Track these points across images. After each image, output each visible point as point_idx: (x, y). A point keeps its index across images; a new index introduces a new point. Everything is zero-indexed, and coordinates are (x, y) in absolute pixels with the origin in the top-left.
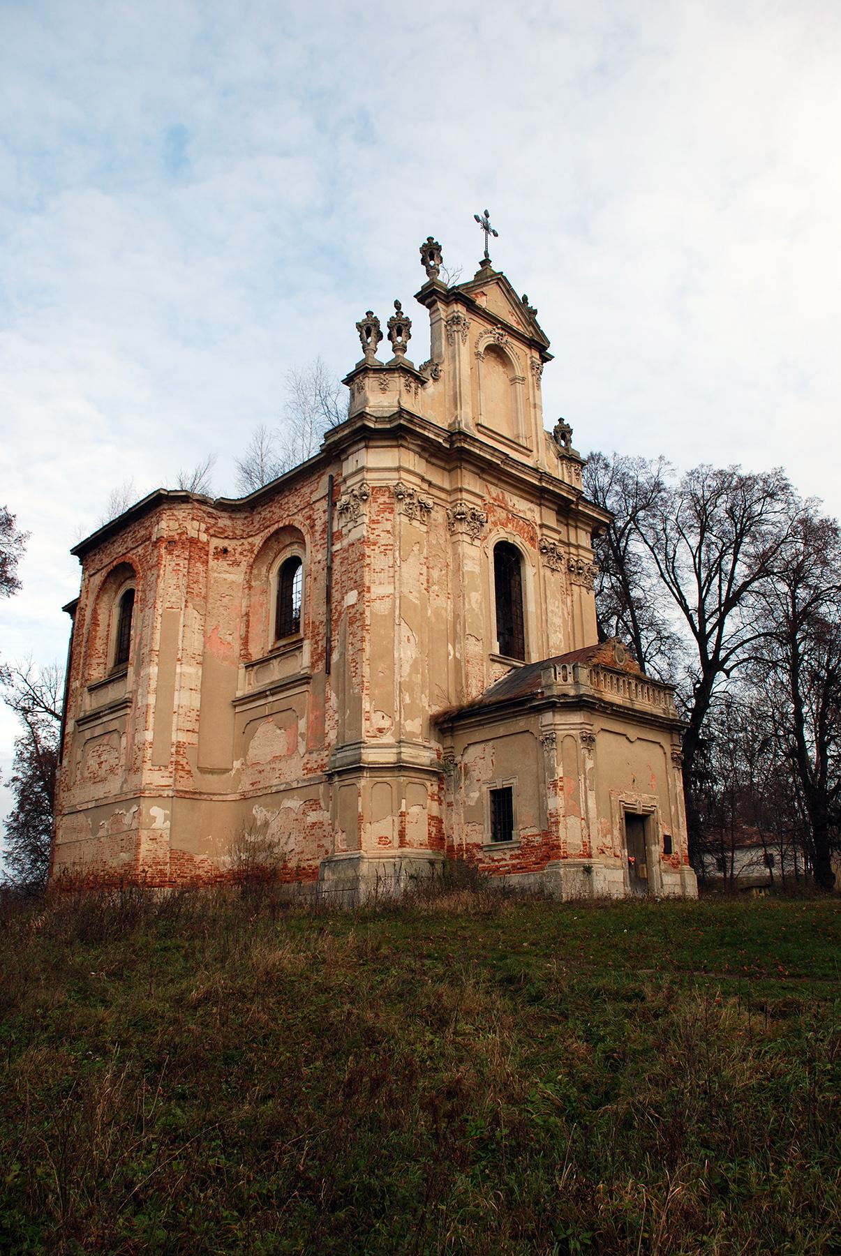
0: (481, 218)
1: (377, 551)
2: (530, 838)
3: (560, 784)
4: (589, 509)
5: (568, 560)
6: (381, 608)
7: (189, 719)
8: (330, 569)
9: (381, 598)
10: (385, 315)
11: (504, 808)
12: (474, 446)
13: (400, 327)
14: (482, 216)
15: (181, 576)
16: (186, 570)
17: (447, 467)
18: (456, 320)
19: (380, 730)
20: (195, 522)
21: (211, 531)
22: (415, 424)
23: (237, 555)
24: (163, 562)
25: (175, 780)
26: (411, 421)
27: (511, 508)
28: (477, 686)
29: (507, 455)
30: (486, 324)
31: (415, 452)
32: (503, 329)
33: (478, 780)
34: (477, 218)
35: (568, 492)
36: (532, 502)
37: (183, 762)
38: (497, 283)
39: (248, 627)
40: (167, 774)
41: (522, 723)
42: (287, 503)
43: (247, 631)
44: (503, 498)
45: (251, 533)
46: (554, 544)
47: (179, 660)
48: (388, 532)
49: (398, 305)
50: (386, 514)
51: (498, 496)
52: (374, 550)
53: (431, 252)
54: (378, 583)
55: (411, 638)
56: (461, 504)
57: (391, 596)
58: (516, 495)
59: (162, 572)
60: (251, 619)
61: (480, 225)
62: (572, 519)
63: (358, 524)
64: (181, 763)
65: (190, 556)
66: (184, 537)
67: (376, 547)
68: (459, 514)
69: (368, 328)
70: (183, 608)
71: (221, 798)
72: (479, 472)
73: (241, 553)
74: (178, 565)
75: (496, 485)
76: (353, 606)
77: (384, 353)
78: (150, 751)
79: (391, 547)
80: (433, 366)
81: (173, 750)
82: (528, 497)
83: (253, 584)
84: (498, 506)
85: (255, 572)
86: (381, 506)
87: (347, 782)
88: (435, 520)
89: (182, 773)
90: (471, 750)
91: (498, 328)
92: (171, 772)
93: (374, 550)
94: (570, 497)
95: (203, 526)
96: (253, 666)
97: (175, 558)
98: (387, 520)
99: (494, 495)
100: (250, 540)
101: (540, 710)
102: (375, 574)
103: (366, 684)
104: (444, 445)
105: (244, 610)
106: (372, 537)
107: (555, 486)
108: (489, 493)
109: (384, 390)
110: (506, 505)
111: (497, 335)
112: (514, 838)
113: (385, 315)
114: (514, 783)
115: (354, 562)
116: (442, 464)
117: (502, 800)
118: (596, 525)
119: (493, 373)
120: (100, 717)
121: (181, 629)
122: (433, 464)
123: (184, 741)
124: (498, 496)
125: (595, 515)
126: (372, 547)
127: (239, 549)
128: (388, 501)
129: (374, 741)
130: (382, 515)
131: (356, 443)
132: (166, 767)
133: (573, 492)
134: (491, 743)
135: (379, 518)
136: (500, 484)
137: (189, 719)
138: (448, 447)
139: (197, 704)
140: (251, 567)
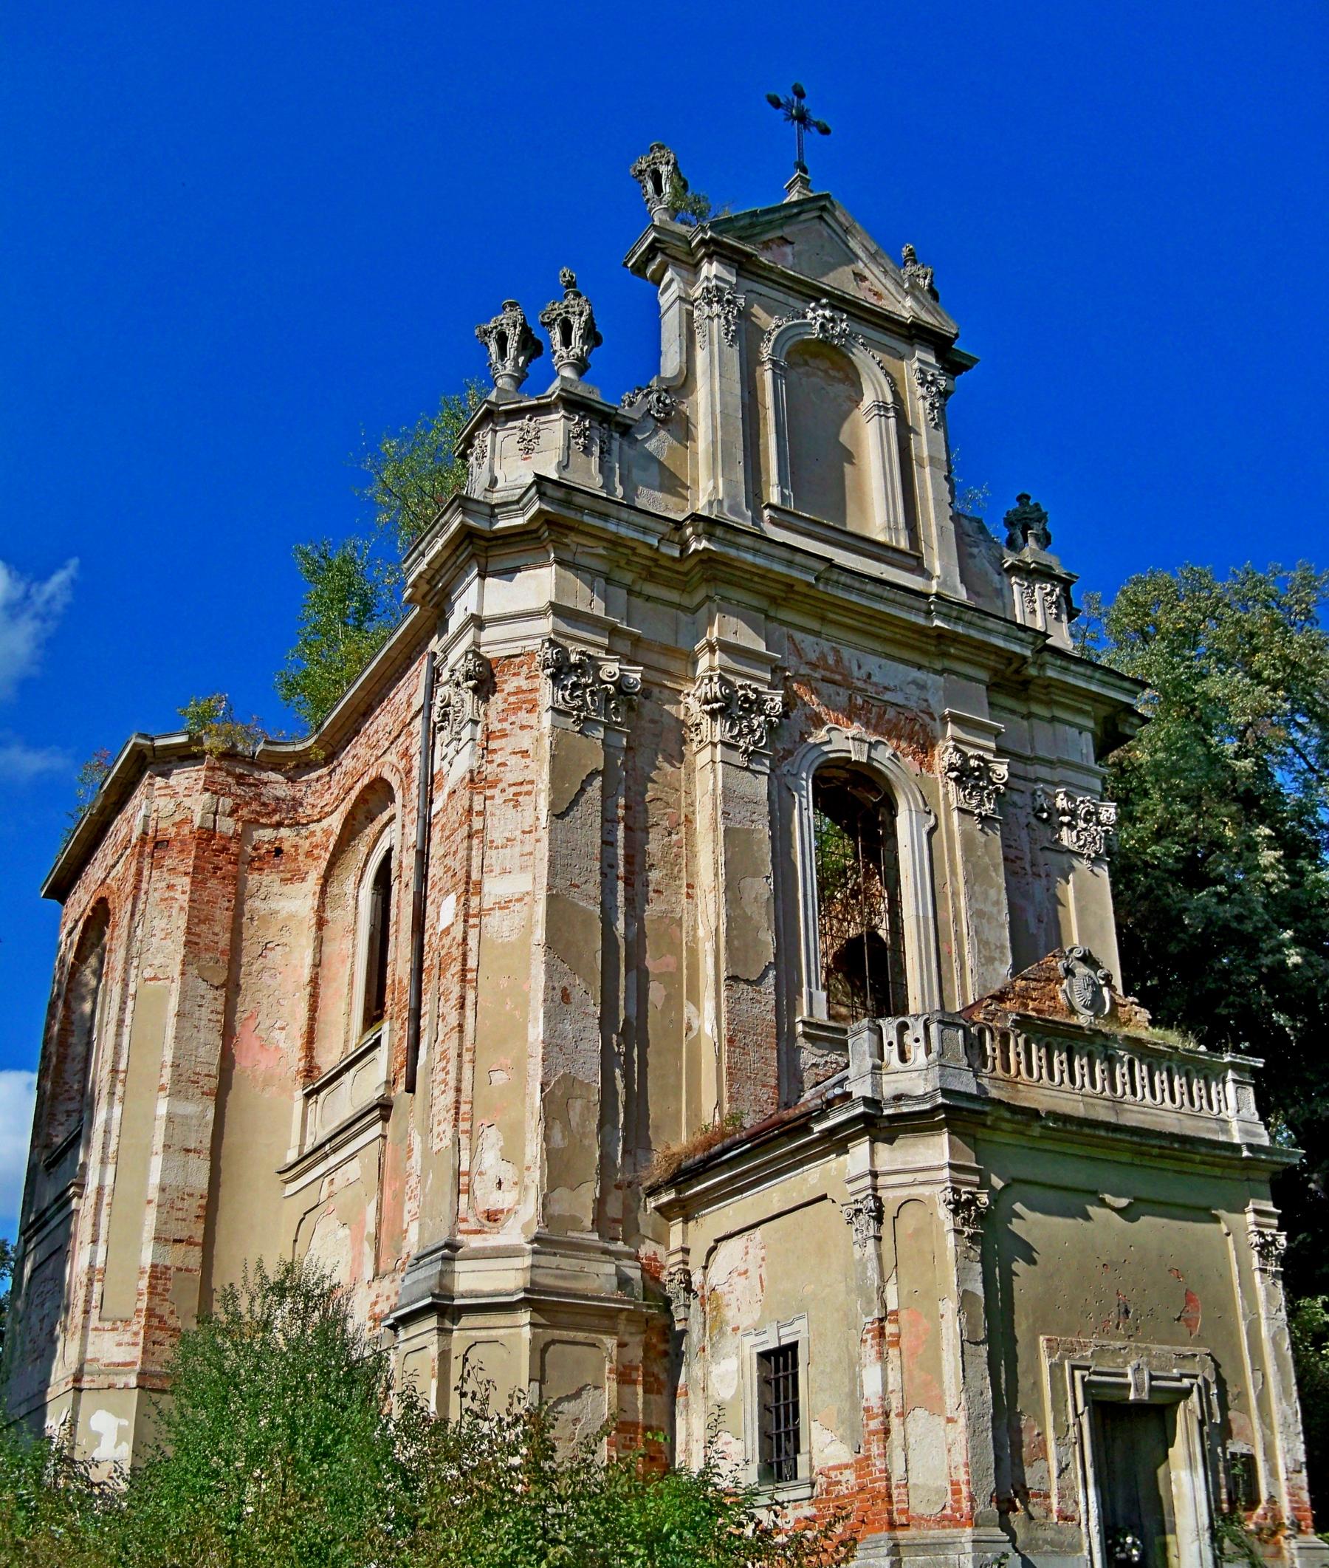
0: (782, 101)
1: (498, 800)
2: (833, 1474)
3: (890, 1328)
4: (1076, 674)
5: (1034, 793)
6: (499, 926)
7: (180, 1214)
8: (423, 857)
9: (504, 905)
11: (786, 1398)
12: (738, 547)
14: (785, 95)
15: (175, 912)
16: (186, 897)
17: (686, 601)
19: (492, 1216)
20: (208, 795)
21: (244, 812)
22: (580, 509)
23: (301, 858)
24: (144, 886)
25: (145, 1351)
26: (567, 503)
27: (860, 684)
28: (757, 1100)
29: (829, 560)
30: (791, 301)
31: (595, 573)
32: (833, 308)
33: (736, 1329)
34: (776, 103)
35: (1006, 637)
36: (920, 667)
37: (164, 1309)
38: (820, 218)
39: (313, 1008)
40: (127, 1338)
41: (812, 1177)
42: (377, 732)
43: (312, 1019)
44: (839, 660)
45: (326, 809)
46: (980, 758)
47: (162, 1088)
48: (524, 753)
50: (522, 714)
51: (823, 657)
52: (492, 798)
54: (497, 870)
55: (577, 994)
56: (711, 679)
57: (527, 899)
58: (874, 652)
59: (141, 906)
60: (322, 991)
61: (780, 113)
62: (1040, 702)
63: (462, 743)
64: (158, 1311)
65: (195, 867)
66: (186, 830)
67: (496, 792)
68: (707, 702)
70: (177, 975)
72: (764, 604)
74: (170, 887)
75: (817, 634)
76: (447, 931)
78: (97, 1287)
79: (526, 788)
81: (144, 1283)
82: (907, 655)
83: (328, 915)
84: (824, 680)
86: (512, 699)
87: (416, 1343)
88: (653, 721)
89: (159, 1335)
91: (823, 307)
92: (136, 1334)
93: (492, 798)
94: (1017, 649)
95: (227, 803)
96: (317, 1091)
97: (166, 875)
98: (522, 727)
99: (813, 657)
100: (325, 823)
101: (837, 1142)
102: (494, 852)
103: (464, 1108)
104: (664, 550)
105: (306, 974)
106: (489, 770)
107: (970, 624)
108: (798, 652)
109: (528, 451)
110: (847, 676)
111: (820, 320)
112: (803, 1473)
115: (455, 830)
116: (674, 596)
118: (1104, 711)
120: (46, 1223)
121: (171, 1021)
122: (648, 598)
123: (168, 1263)
124: (823, 657)
125: (1094, 688)
126: (488, 792)
127: (306, 845)
128: (525, 684)
130: (512, 718)
131: (462, 571)
132: (127, 1322)
133: (1021, 635)
134: (758, 1233)
135: (506, 725)
136: (827, 630)
137: (180, 1214)
138: (677, 554)
139: (201, 1181)
140: (326, 879)
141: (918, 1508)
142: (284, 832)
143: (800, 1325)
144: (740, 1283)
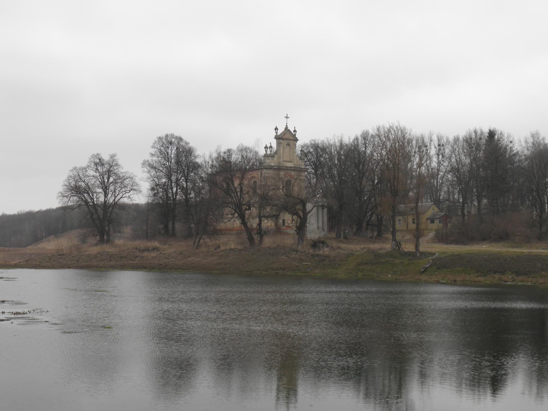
10: (268, 146)
13: (271, 147)
18: (280, 143)
49: (270, 143)
53: (276, 129)
69: (266, 147)
77: (269, 152)
80: (276, 153)
113: (268, 146)
114: (285, 219)
117: (284, 220)
119: (287, 149)
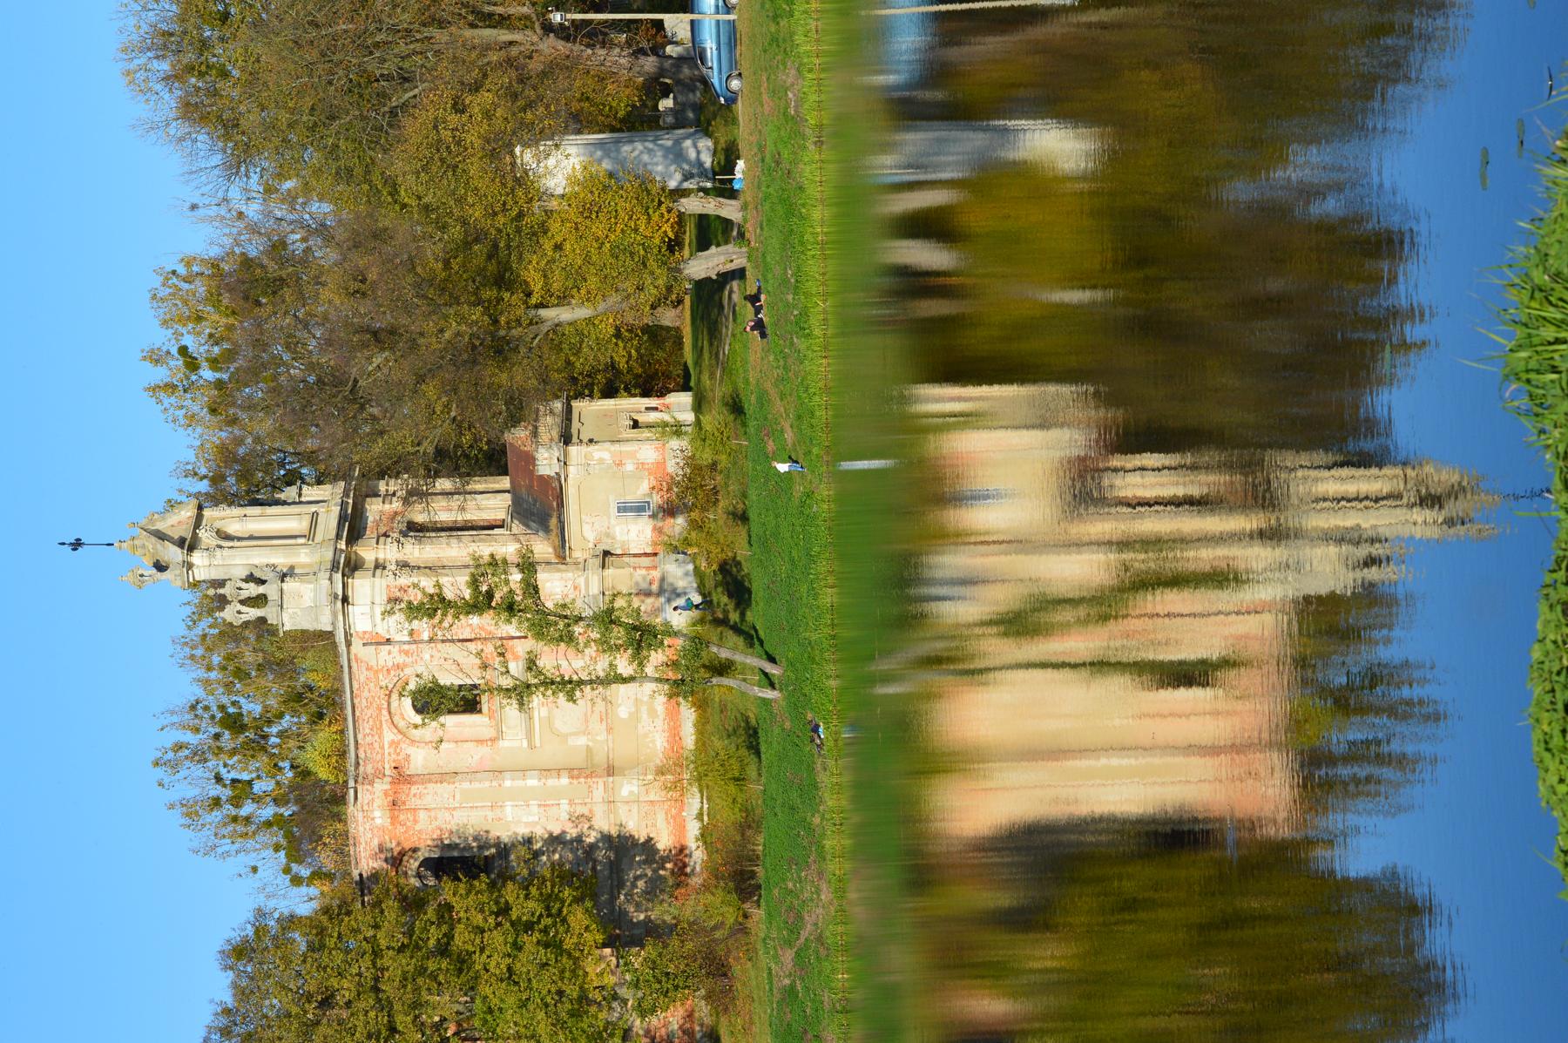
15: (426, 791)
19: (575, 588)
40: (595, 786)
47: (500, 785)
71: (611, 752)
73: (398, 754)
81: (575, 781)
85: (417, 739)
90: (585, 534)
100: (386, 746)
127: (393, 756)
129: (583, 592)
141: (661, 457)
142: (387, 766)
143: (611, 498)
144: (597, 526)
